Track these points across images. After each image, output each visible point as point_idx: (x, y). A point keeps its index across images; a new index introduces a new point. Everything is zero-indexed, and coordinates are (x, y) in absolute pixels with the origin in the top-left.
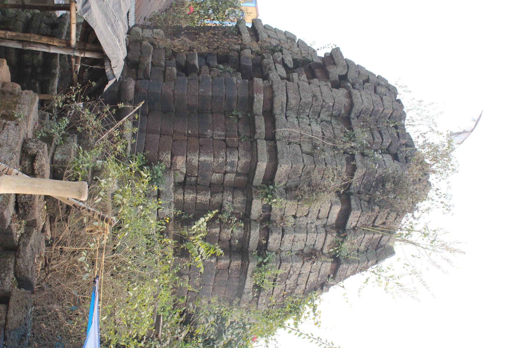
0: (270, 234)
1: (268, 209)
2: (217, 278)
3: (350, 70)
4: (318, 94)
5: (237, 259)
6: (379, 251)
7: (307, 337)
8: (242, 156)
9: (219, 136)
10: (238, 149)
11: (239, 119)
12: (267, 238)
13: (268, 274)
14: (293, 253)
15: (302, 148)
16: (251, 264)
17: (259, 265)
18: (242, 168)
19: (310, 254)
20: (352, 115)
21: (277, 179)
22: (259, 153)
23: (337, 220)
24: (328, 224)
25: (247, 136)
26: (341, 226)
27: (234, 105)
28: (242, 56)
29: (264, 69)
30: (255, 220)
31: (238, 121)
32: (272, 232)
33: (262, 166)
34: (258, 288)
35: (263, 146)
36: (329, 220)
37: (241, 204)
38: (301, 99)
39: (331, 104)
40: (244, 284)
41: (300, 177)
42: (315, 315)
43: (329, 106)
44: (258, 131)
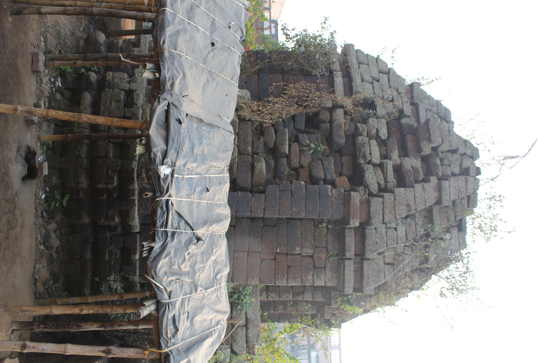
4: (412, 203)
10: (325, 268)
22: (346, 280)
28: (335, 123)
29: (358, 153)
35: (350, 267)
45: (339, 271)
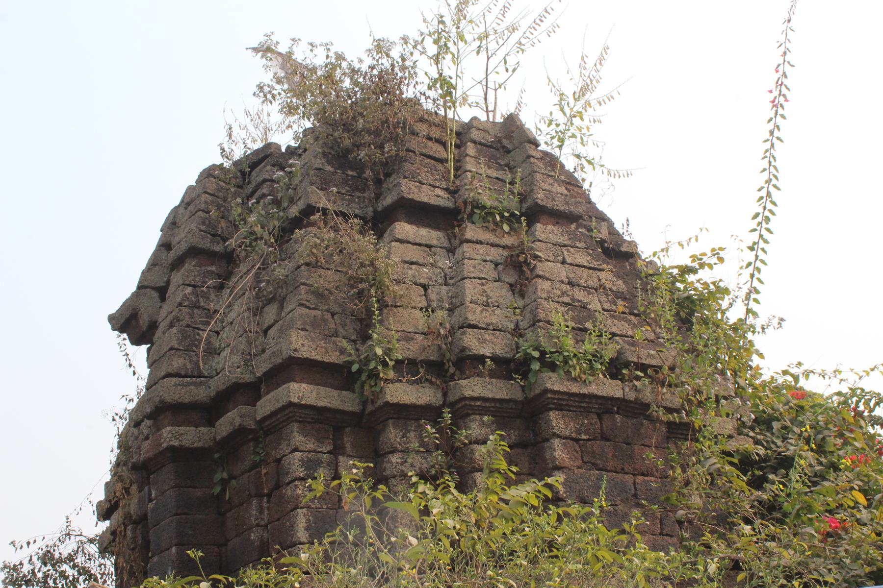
0: (468, 353)
1: (408, 367)
2: (611, 465)
3: (146, 284)
5: (548, 422)
6: (509, 142)
7: (756, 274)
8: (288, 445)
9: (261, 511)
11: (232, 477)
12: (481, 359)
13: (569, 342)
14: (520, 303)
15: (272, 321)
16: (549, 386)
17: (553, 367)
18: (320, 440)
19: (519, 269)
20: (218, 248)
21: (334, 358)
23: (436, 227)
24: (446, 244)
25: (256, 447)
26: (446, 218)
27: (199, 493)
30: (445, 395)
31: (235, 478)
32: (463, 349)
33: (301, 391)
34: (616, 368)
35: (267, 404)
36: (435, 242)
37: (409, 431)
38: (172, 349)
39: (189, 290)
40: (612, 399)
41: (333, 315)
42: (702, 266)
43: (193, 293)
44: (238, 421)
45: (273, 427)
